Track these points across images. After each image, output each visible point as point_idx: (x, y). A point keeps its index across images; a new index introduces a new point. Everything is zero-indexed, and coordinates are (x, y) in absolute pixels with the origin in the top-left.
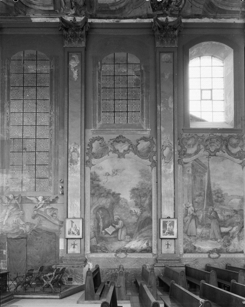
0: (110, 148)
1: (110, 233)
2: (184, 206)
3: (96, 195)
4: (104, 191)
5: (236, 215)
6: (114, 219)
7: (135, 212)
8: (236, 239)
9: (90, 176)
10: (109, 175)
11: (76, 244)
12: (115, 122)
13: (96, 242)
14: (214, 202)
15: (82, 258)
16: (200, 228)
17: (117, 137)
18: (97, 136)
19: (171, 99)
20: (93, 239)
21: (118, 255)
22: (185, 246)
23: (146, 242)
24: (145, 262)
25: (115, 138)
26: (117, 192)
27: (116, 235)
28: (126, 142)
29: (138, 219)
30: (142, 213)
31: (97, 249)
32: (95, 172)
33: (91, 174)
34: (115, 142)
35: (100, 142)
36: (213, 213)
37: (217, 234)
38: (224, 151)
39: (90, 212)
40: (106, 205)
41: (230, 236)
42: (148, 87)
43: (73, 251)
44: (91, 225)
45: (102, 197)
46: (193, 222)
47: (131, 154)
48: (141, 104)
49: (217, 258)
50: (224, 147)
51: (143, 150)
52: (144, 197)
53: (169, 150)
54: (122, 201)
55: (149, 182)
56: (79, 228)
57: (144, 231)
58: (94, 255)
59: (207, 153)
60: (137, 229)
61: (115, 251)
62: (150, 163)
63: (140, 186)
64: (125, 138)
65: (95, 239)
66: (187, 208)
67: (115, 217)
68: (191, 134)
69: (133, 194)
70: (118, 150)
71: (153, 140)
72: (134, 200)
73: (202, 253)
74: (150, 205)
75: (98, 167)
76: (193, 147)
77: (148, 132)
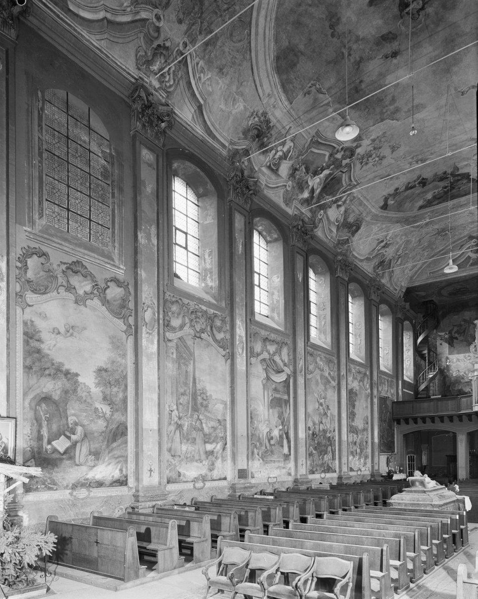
0: (61, 280)
4: (49, 365)
5: (220, 427)
6: (67, 424)
7: (103, 412)
8: (220, 460)
9: (23, 328)
10: (59, 333)
12: (70, 231)
14: (199, 406)
18: (37, 246)
19: (153, 230)
21: (74, 493)
23: (119, 467)
25: (70, 262)
28: (89, 278)
29: (108, 424)
30: (112, 415)
32: (32, 322)
33: (25, 323)
35: (42, 260)
37: (202, 453)
38: (209, 334)
39: (23, 405)
42: (121, 190)
46: (178, 432)
47: (96, 302)
48: (111, 216)
50: (209, 328)
51: (114, 301)
52: (115, 387)
54: (82, 388)
55: (124, 361)
59: (192, 332)
61: (71, 485)
62: (125, 328)
64: (86, 268)
67: (69, 419)
69: (99, 379)
70: (74, 288)
73: (187, 482)
74: (125, 400)
76: (177, 317)
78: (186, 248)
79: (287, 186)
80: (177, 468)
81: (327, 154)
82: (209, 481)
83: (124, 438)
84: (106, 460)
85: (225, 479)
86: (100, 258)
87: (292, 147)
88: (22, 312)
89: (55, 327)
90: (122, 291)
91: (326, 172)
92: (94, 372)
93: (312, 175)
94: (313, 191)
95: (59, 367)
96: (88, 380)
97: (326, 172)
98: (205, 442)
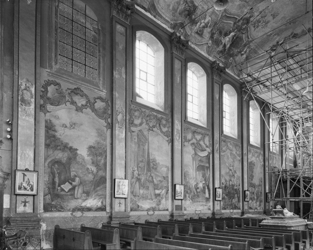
0: (67, 98)
1: (67, 190)
2: (132, 170)
3: (51, 146)
4: (60, 144)
5: (164, 181)
6: (70, 176)
7: (92, 170)
8: (164, 200)
9: (45, 124)
10: (66, 127)
11: (27, 201)
12: (73, 71)
13: (51, 200)
14: (151, 169)
15: (36, 218)
16: (142, 189)
17: (75, 89)
18: (53, 80)
19: (123, 70)
20: (47, 196)
21: (74, 214)
22: (131, 204)
23: (101, 201)
24: (100, 220)
25: (73, 88)
26: (75, 147)
27: (73, 193)
28: (84, 97)
29: (94, 177)
30: (97, 172)
31: (51, 207)
32: (50, 120)
33: (46, 121)
34: (73, 93)
35: (57, 87)
36: (150, 178)
37: (153, 195)
38: (158, 128)
39: (44, 165)
40: (62, 159)
41: (160, 197)
42: (104, 49)
43: (24, 210)
44: (45, 180)
45: (58, 150)
46: (138, 183)
47: (89, 110)
48: (98, 63)
49: (153, 215)
50: (158, 125)
51: (99, 110)
52: (99, 156)
53: (122, 117)
54: (80, 157)
55: (105, 143)
56: (33, 183)
57: (99, 190)
58: (48, 215)
59: (147, 127)
60: (93, 187)
61: (72, 209)
62: (106, 124)
63: (96, 145)
64: (83, 91)
65: (50, 196)
66: (133, 172)
67: (72, 173)
68: (137, 107)
69: (90, 152)
70: (76, 103)
71: (108, 103)
72: (91, 158)
73: (143, 211)
74: (105, 164)
75: (54, 116)
76: (138, 119)
77: (104, 93)
78: (146, 81)
79: (209, 44)
80: (137, 203)
81: (232, 22)
82: (157, 211)
83: (105, 185)
84: (93, 196)
85: (167, 210)
86: (91, 86)
87: (210, 20)
88: (44, 115)
89: (64, 123)
90: (104, 104)
91: (232, 34)
92: (87, 148)
93: (224, 36)
94: (225, 46)
95: (66, 145)
96: (83, 152)
97: (232, 34)
98: (155, 189)
